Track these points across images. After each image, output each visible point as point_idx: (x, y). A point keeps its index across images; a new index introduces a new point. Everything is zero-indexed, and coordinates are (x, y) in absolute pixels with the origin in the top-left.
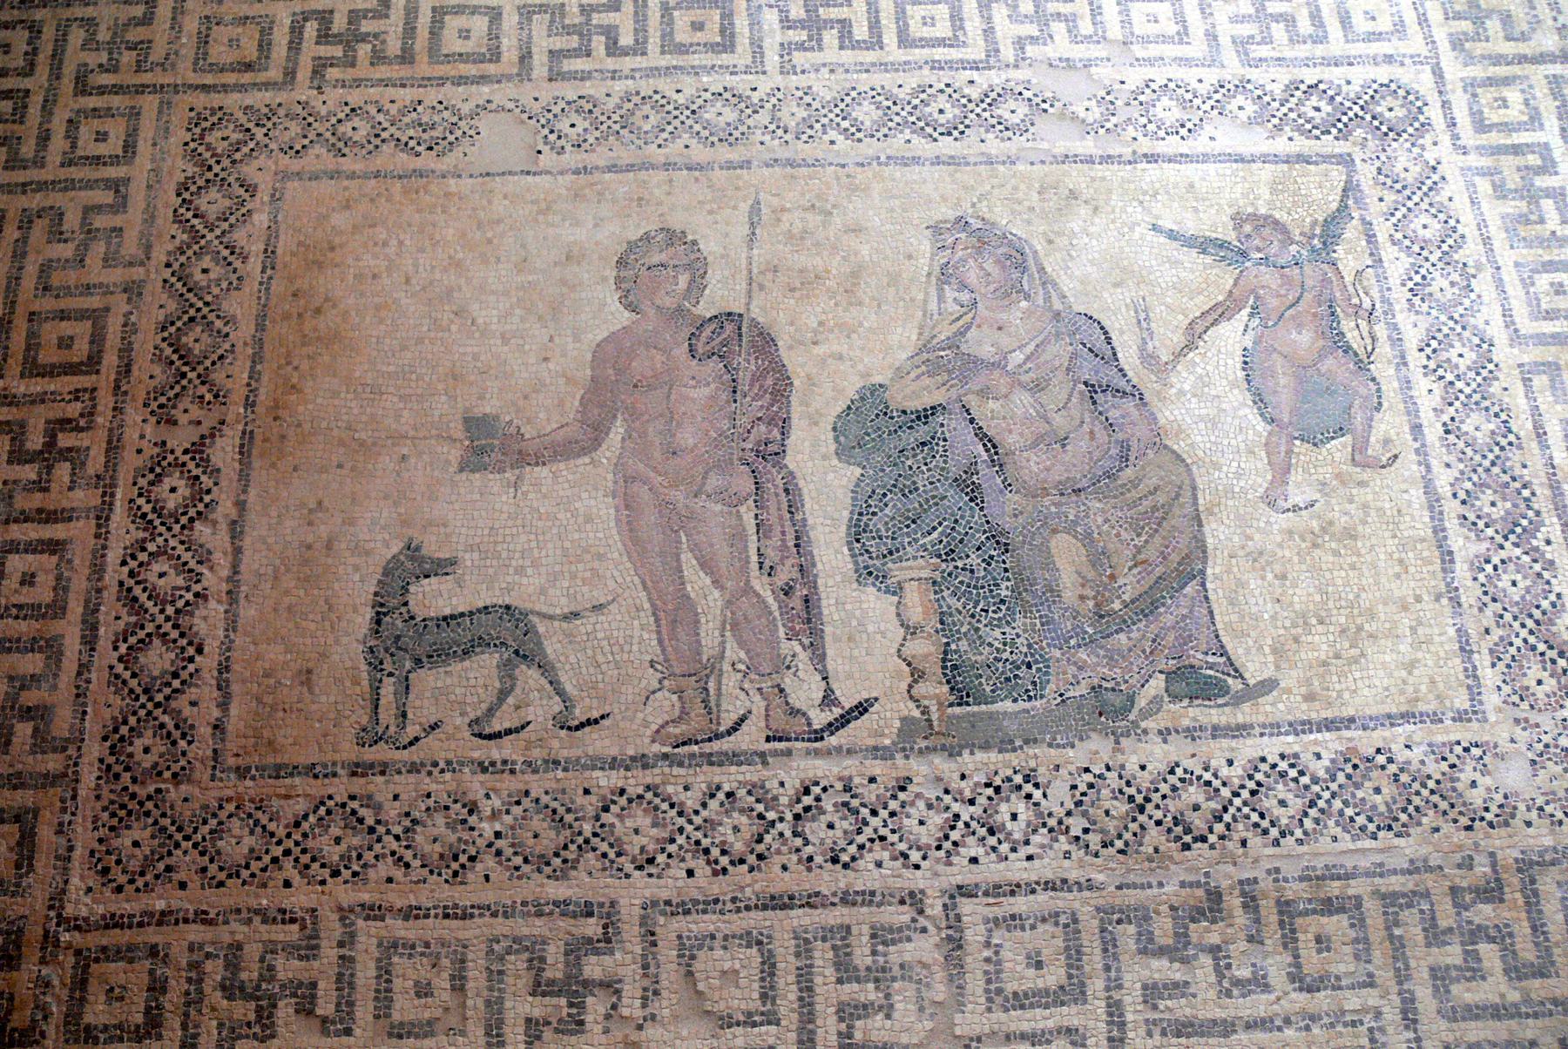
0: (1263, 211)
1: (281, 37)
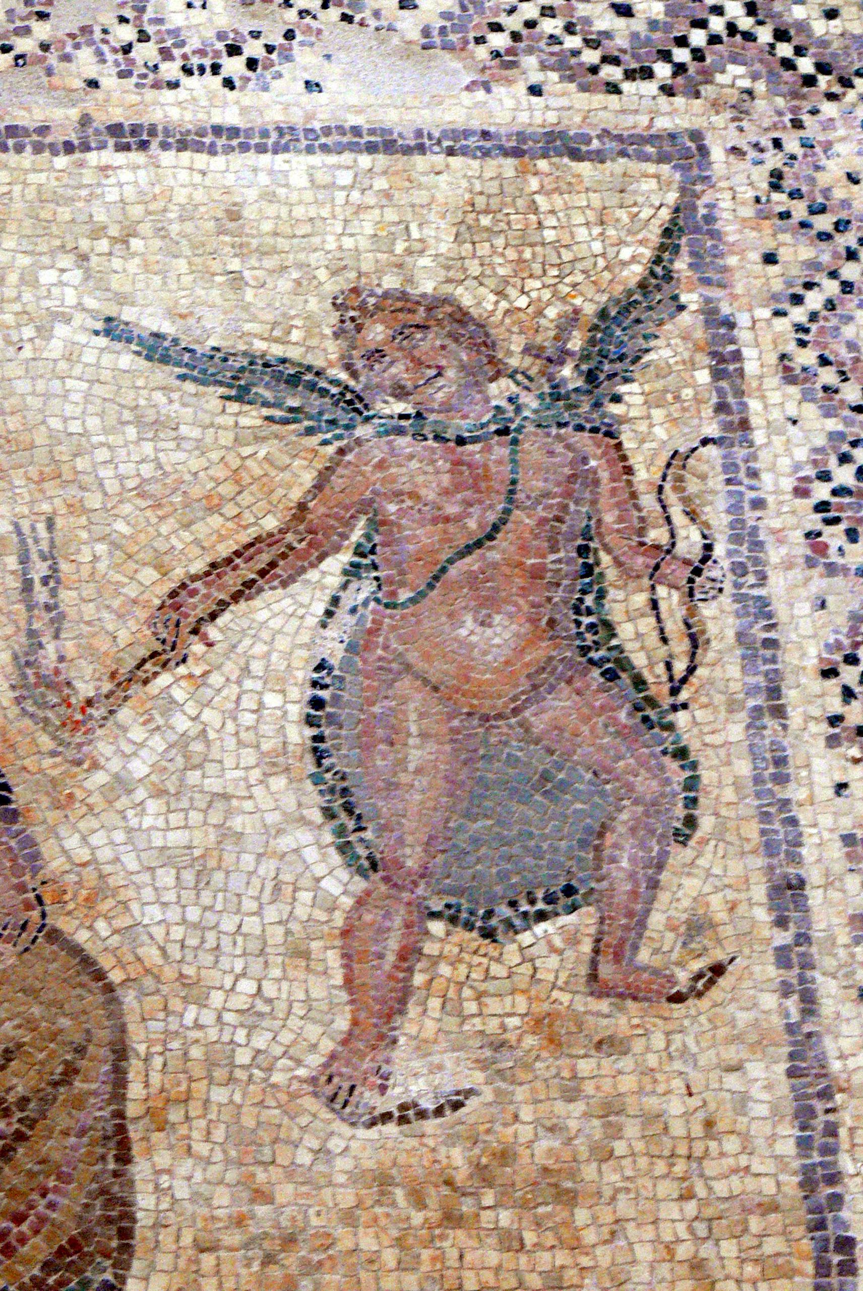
0: (427, 286)
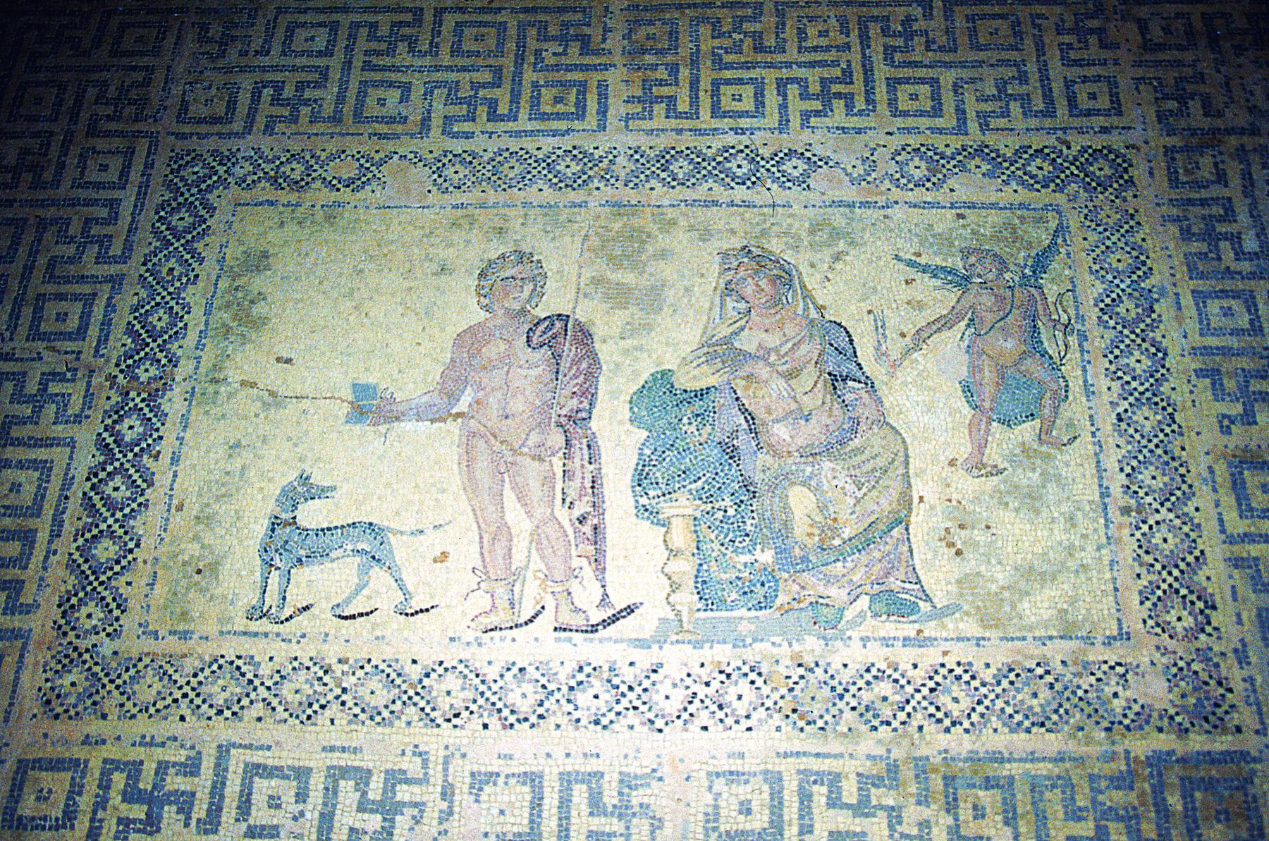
1: (244, 98)
